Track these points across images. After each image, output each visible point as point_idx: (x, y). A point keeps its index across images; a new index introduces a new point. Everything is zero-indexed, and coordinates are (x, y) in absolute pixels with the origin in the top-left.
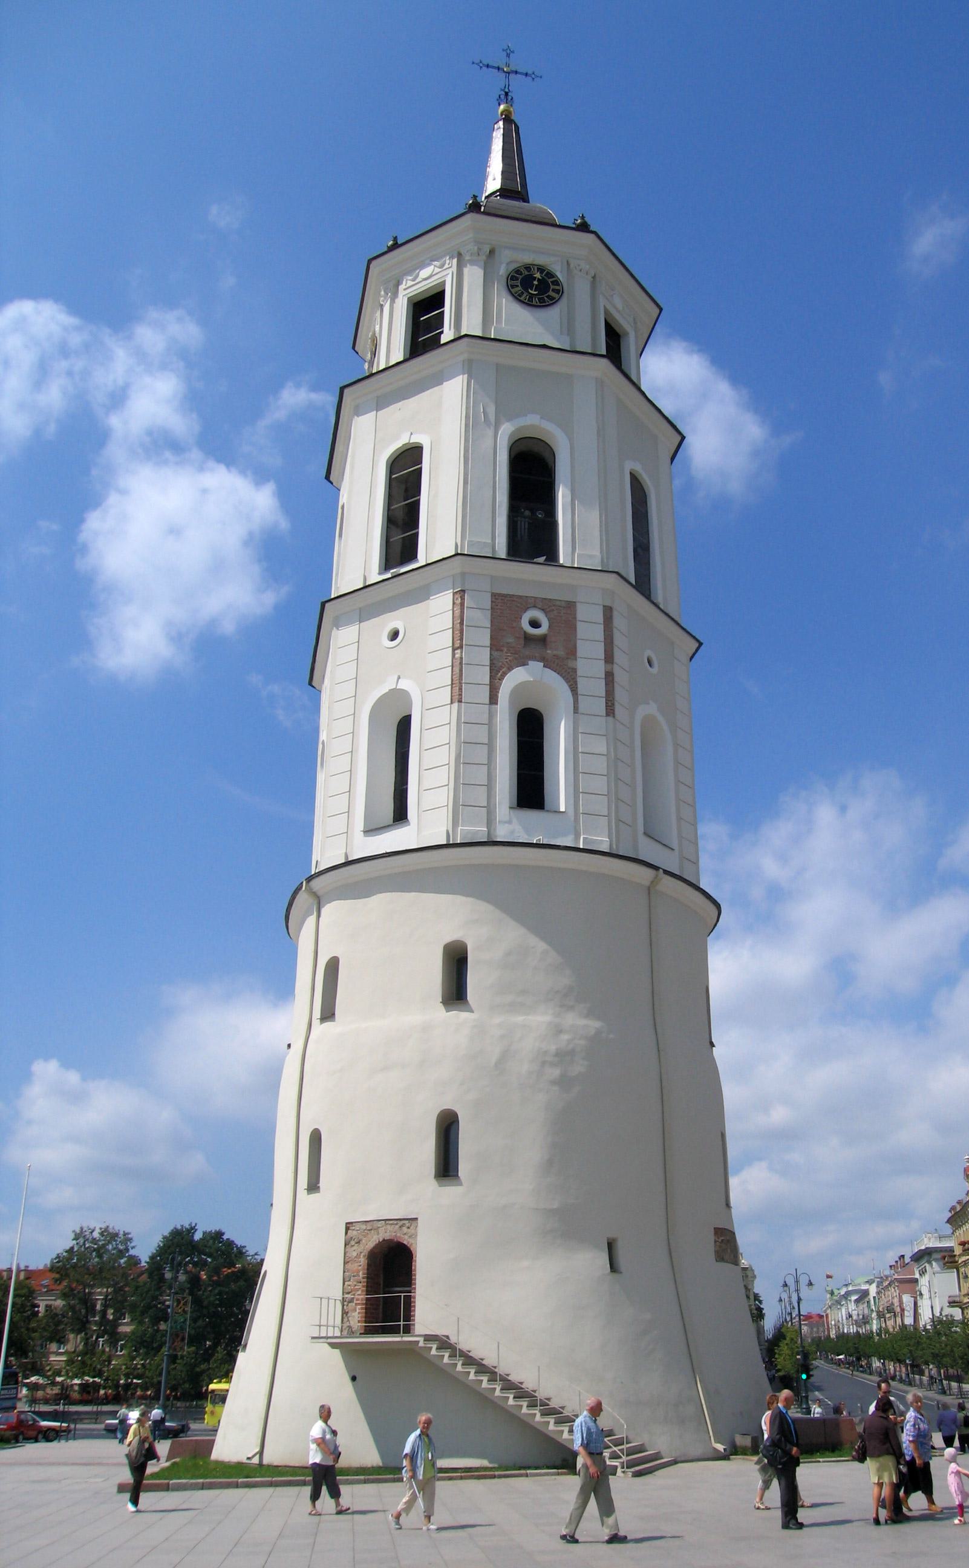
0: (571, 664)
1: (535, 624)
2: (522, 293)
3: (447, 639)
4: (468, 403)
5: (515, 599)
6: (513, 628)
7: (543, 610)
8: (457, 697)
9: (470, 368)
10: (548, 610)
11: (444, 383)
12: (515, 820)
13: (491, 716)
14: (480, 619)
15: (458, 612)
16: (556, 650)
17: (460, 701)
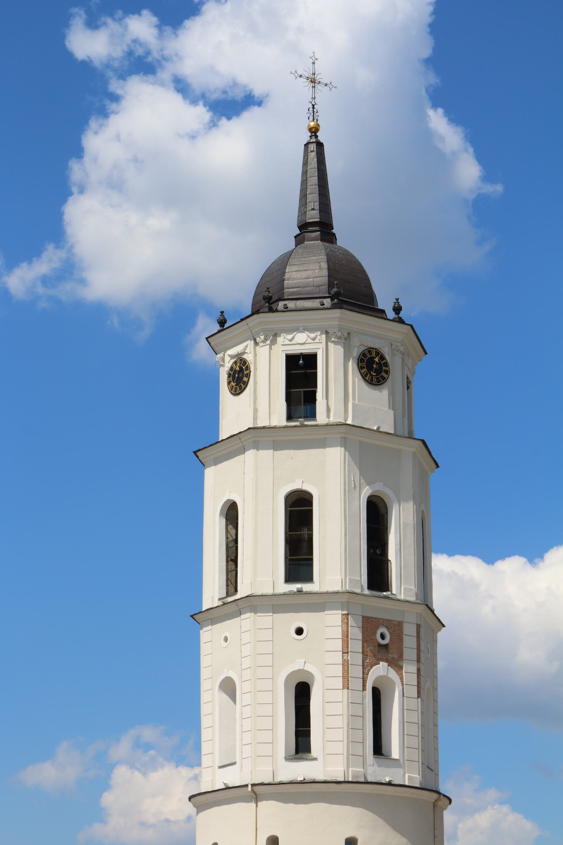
0: (400, 663)
1: (383, 637)
2: (367, 374)
3: (338, 645)
4: (345, 472)
5: (373, 620)
6: (372, 639)
7: (387, 627)
8: (346, 686)
9: (344, 443)
10: (389, 627)
11: (326, 448)
12: (376, 765)
13: (363, 698)
14: (356, 633)
15: (345, 628)
16: (393, 655)
17: (348, 689)
